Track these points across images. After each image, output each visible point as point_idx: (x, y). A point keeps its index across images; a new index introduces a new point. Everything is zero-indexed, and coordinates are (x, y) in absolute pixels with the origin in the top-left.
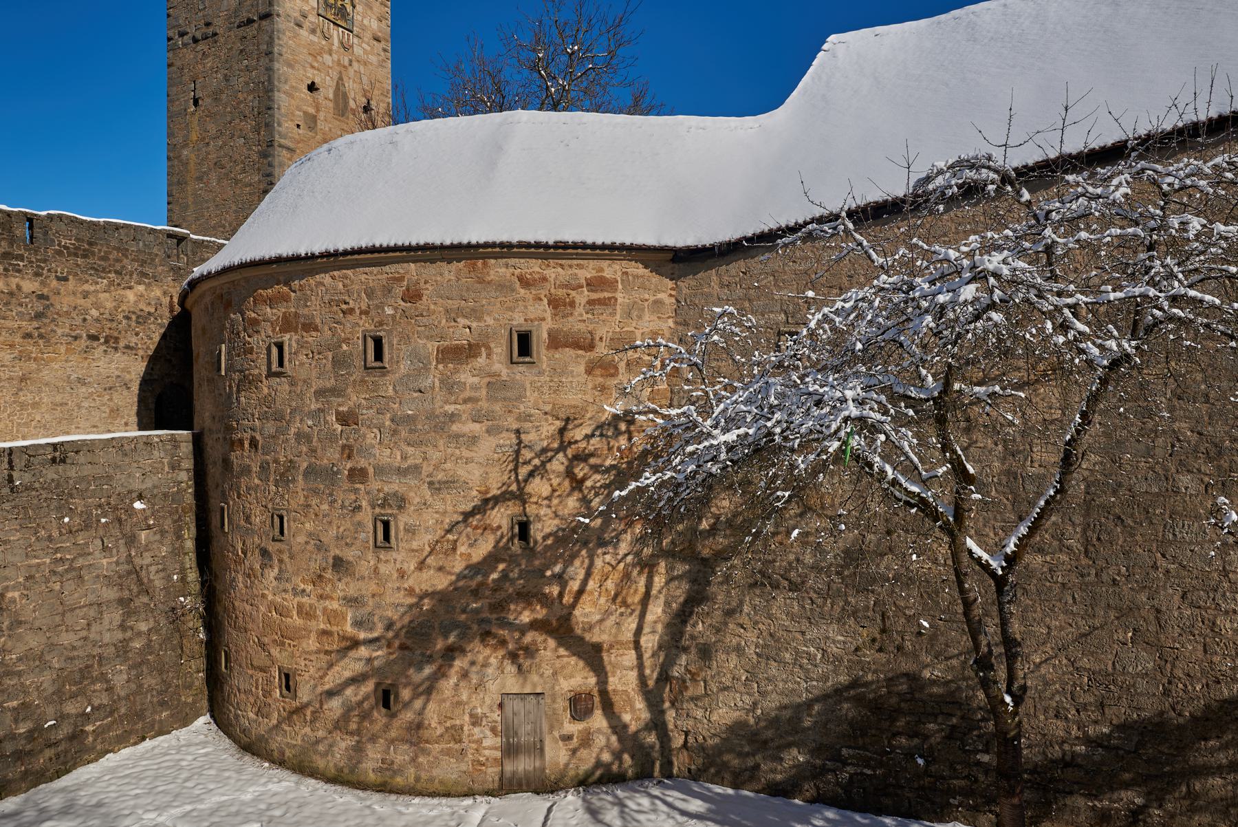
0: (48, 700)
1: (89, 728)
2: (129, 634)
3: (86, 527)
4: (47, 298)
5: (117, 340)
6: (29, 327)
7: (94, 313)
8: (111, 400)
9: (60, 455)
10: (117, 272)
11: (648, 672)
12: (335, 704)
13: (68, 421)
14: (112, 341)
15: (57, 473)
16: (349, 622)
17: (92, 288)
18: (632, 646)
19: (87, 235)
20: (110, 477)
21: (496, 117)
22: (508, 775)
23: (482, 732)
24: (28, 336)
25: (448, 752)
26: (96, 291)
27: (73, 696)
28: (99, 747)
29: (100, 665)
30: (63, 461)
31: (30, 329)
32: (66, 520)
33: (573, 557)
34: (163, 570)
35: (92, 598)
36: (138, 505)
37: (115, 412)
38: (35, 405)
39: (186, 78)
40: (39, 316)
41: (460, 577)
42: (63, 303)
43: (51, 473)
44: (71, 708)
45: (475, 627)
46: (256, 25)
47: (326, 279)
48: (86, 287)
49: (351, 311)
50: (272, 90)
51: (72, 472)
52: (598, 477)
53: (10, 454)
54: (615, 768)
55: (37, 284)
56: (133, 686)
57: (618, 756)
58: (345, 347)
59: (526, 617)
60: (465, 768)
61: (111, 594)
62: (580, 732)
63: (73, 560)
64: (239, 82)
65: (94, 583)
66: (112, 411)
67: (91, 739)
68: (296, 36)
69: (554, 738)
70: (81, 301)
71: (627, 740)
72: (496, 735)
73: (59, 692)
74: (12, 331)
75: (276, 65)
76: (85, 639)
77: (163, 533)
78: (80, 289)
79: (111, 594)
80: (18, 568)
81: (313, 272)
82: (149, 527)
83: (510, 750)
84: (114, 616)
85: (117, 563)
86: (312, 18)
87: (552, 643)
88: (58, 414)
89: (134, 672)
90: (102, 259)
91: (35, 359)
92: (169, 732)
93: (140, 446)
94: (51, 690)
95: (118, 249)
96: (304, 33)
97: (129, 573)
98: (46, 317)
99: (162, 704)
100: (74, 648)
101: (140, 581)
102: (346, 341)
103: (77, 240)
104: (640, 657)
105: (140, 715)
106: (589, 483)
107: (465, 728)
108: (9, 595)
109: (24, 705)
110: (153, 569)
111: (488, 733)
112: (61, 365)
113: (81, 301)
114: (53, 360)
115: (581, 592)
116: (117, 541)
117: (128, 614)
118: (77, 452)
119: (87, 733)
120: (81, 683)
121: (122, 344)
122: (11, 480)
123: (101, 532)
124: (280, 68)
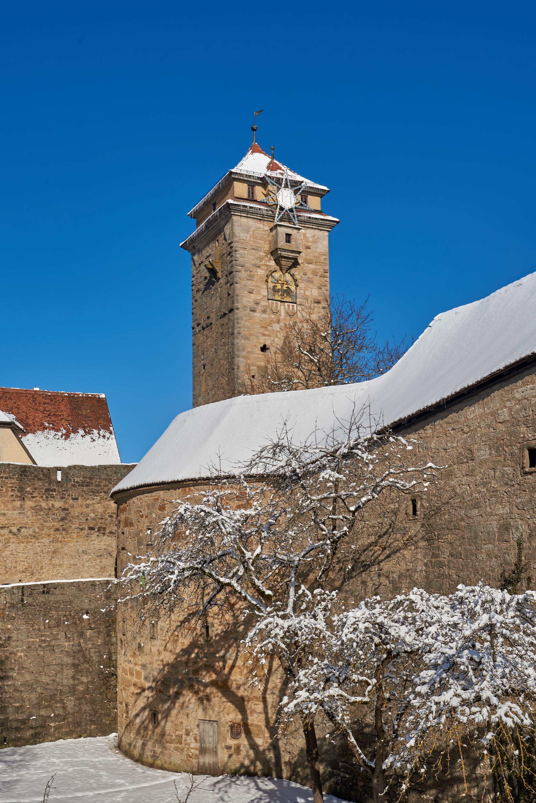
0: (33, 707)
1: (52, 724)
2: (76, 682)
3: (58, 626)
4: (67, 510)
5: (104, 529)
6: (57, 525)
7: (92, 515)
8: (101, 562)
9: (47, 589)
10: (105, 492)
11: (270, 715)
12: (138, 720)
13: (78, 573)
14: (102, 530)
15: (45, 598)
16: (143, 677)
17: (91, 502)
18: (261, 699)
19: (88, 474)
20: (71, 602)
21: (228, 400)
22: (201, 764)
23: (190, 739)
24: (57, 530)
25: (176, 749)
26: (93, 504)
27: (46, 707)
28: (56, 735)
29: (61, 695)
30: (48, 592)
31: (58, 526)
32: (47, 621)
33: (230, 647)
34: (99, 652)
35: (58, 661)
36: (85, 617)
37: (103, 569)
38: (61, 565)
39: (200, 352)
40: (63, 519)
41: (178, 655)
42: (75, 512)
43: (41, 598)
44: (43, 712)
45: (186, 681)
46: (227, 316)
47: (135, 499)
48: (88, 502)
49: (143, 515)
50: (233, 358)
51: (52, 598)
52: (240, 603)
53: (23, 589)
54: (252, 768)
55: (62, 503)
56: (77, 709)
57: (253, 762)
58: (141, 534)
59: (207, 680)
60: (183, 758)
61: (69, 660)
62: (235, 745)
63: (50, 641)
64: (221, 353)
65: (60, 654)
66: (101, 568)
67: (53, 730)
68: (251, 318)
69: (222, 747)
70: (85, 510)
71: (259, 755)
72: (196, 742)
73: (39, 704)
74: (49, 528)
75: (236, 341)
76: (54, 681)
77: (99, 632)
78: (85, 503)
79: (69, 660)
80: (23, 642)
81: (131, 497)
82: (91, 629)
83: (203, 751)
84: (70, 672)
85: (73, 645)
86: (264, 303)
87: (220, 694)
88: (72, 570)
89: (78, 702)
90: (97, 486)
91: (61, 542)
92: (95, 737)
93: (89, 586)
94: (35, 702)
95: (105, 480)
96: (257, 314)
97: (79, 651)
98: (66, 520)
99: (93, 722)
100: (48, 684)
101: (84, 656)
102: (141, 531)
103: (84, 477)
104: (265, 707)
105: (79, 724)
106: (237, 606)
107: (183, 736)
108: (19, 654)
109: (21, 706)
110: (92, 651)
111: (193, 740)
112: (74, 544)
113: (85, 510)
114: (70, 542)
115: (233, 667)
116: (73, 634)
117: (77, 672)
118: (55, 589)
119: (51, 727)
120: (50, 702)
121: (107, 531)
122: (22, 600)
123: (65, 629)
124: (240, 342)
